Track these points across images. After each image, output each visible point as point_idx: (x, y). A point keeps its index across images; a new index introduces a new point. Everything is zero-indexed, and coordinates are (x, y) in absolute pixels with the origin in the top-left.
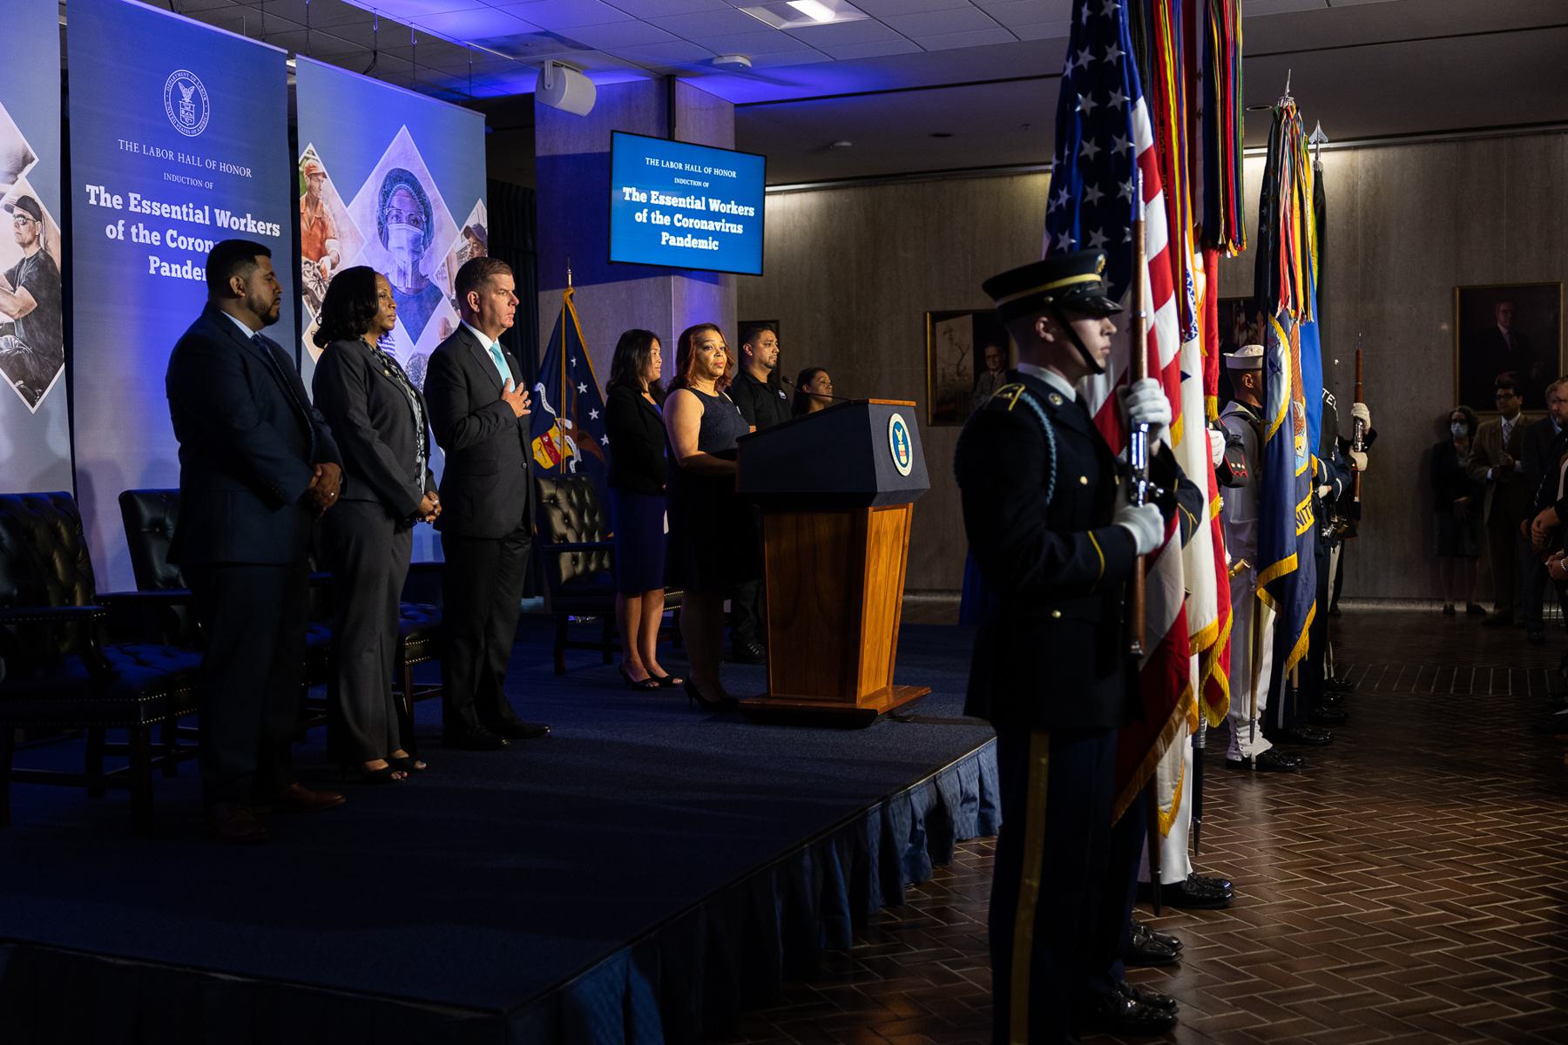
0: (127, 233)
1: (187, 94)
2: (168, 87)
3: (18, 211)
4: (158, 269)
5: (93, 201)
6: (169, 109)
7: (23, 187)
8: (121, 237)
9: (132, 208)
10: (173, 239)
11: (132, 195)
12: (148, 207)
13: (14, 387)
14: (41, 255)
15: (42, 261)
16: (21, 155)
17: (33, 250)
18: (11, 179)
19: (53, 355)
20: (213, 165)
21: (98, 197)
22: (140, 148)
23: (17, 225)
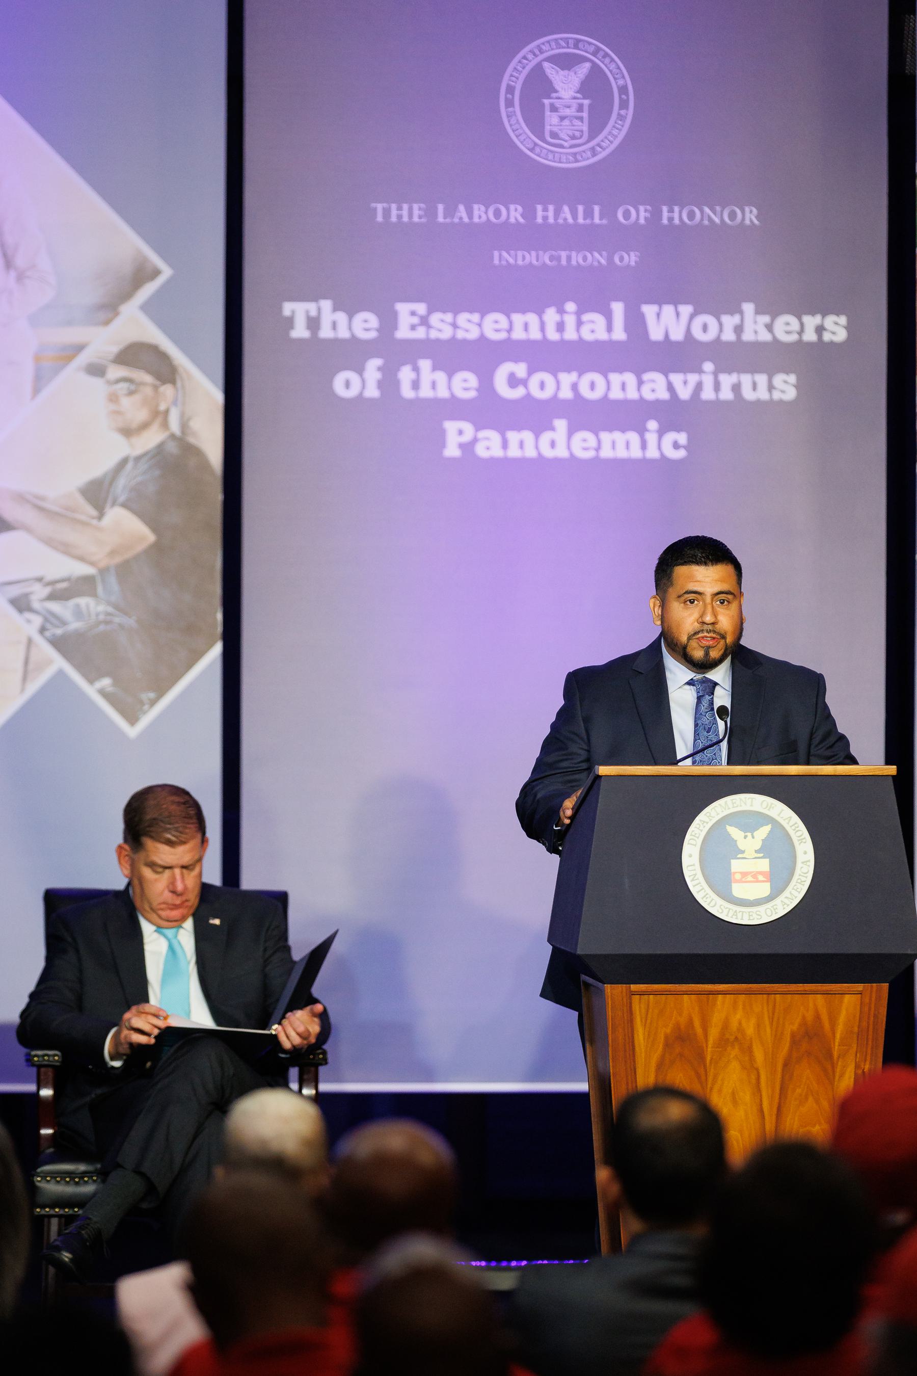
0: (389, 382)
1: (566, 84)
2: (515, 74)
3: (116, 372)
4: (468, 448)
5: (300, 331)
6: (514, 125)
7: (134, 324)
8: (372, 392)
9: (403, 332)
10: (513, 381)
11: (403, 309)
12: (441, 326)
13: (91, 691)
14: (172, 448)
15: (174, 460)
17: (152, 439)
20: (642, 214)
21: (313, 323)
22: (431, 213)
23: (113, 398)
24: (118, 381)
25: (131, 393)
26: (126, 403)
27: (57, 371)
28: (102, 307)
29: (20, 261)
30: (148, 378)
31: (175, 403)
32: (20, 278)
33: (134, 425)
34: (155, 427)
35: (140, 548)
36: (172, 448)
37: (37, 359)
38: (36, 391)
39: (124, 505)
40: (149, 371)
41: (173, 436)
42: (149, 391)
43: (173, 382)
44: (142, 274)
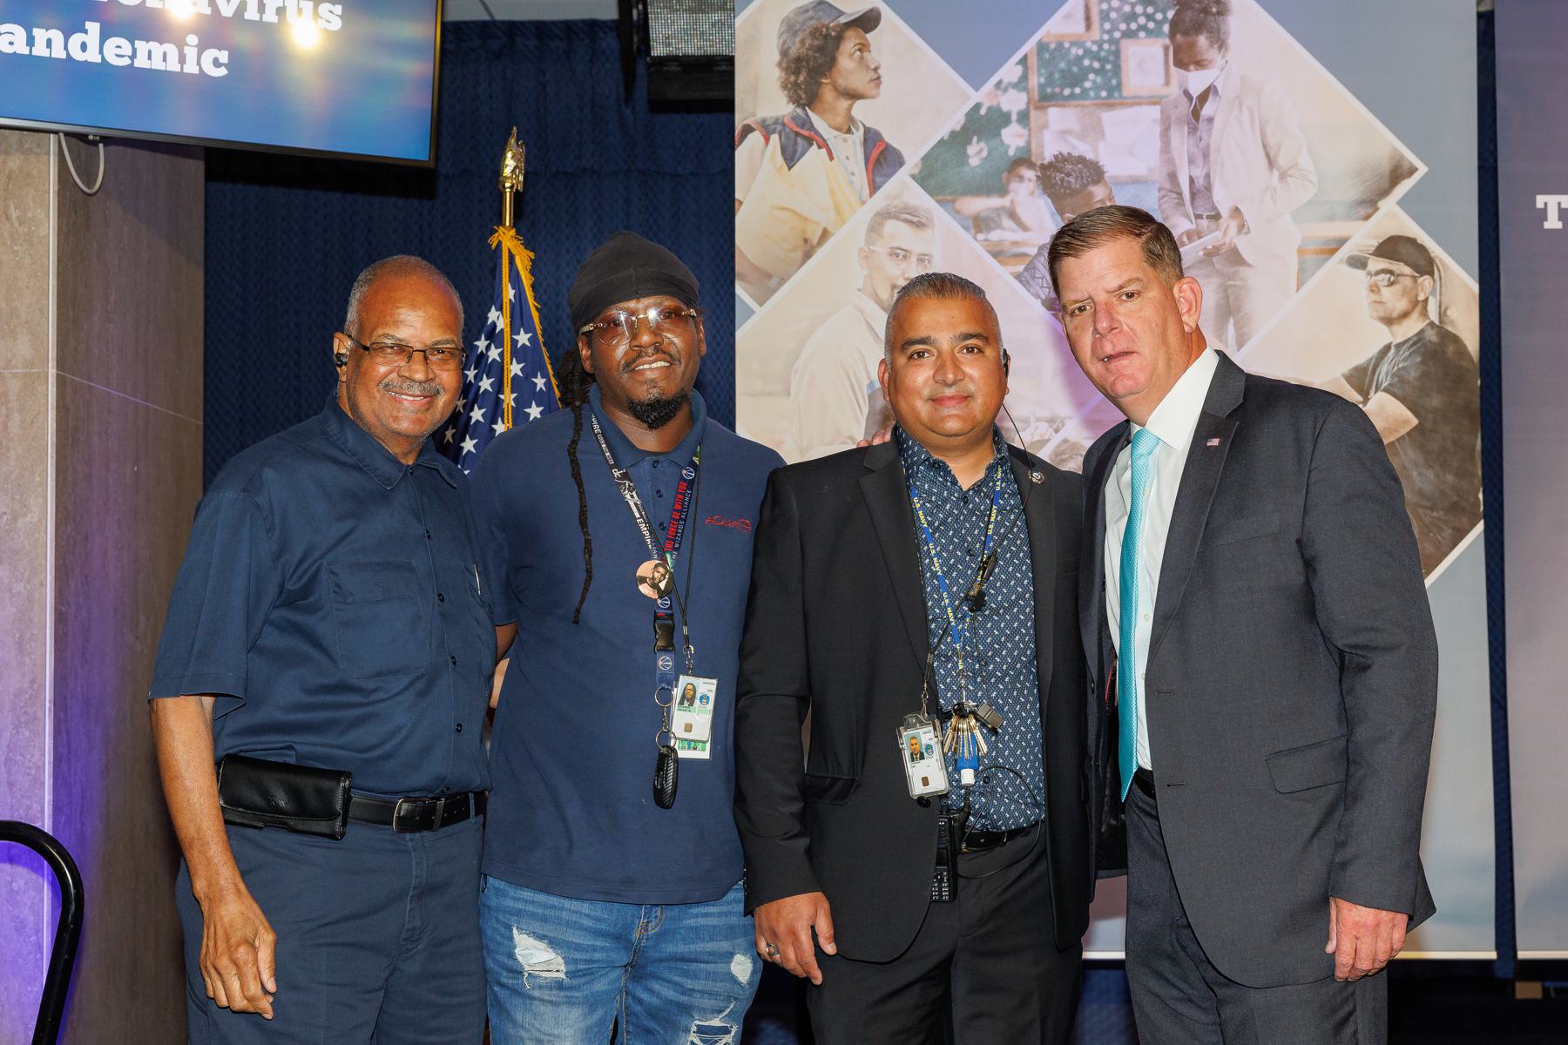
3: (1376, 264)
7: (1393, 218)
14: (1431, 336)
15: (1435, 349)
16: (1386, 167)
17: (1412, 327)
18: (1363, 211)
19: (1455, 508)
23: (1374, 289)
24: (1378, 273)
25: (1391, 284)
26: (1386, 292)
27: (1320, 265)
28: (1362, 202)
29: (1282, 161)
30: (1407, 270)
31: (1433, 293)
32: (1283, 177)
33: (1395, 315)
34: (1415, 315)
35: (1404, 431)
36: (1431, 336)
37: (1301, 252)
38: (1300, 283)
39: (1385, 390)
40: (1407, 263)
41: (1432, 324)
42: (1408, 282)
43: (1431, 274)
44: (1398, 173)
